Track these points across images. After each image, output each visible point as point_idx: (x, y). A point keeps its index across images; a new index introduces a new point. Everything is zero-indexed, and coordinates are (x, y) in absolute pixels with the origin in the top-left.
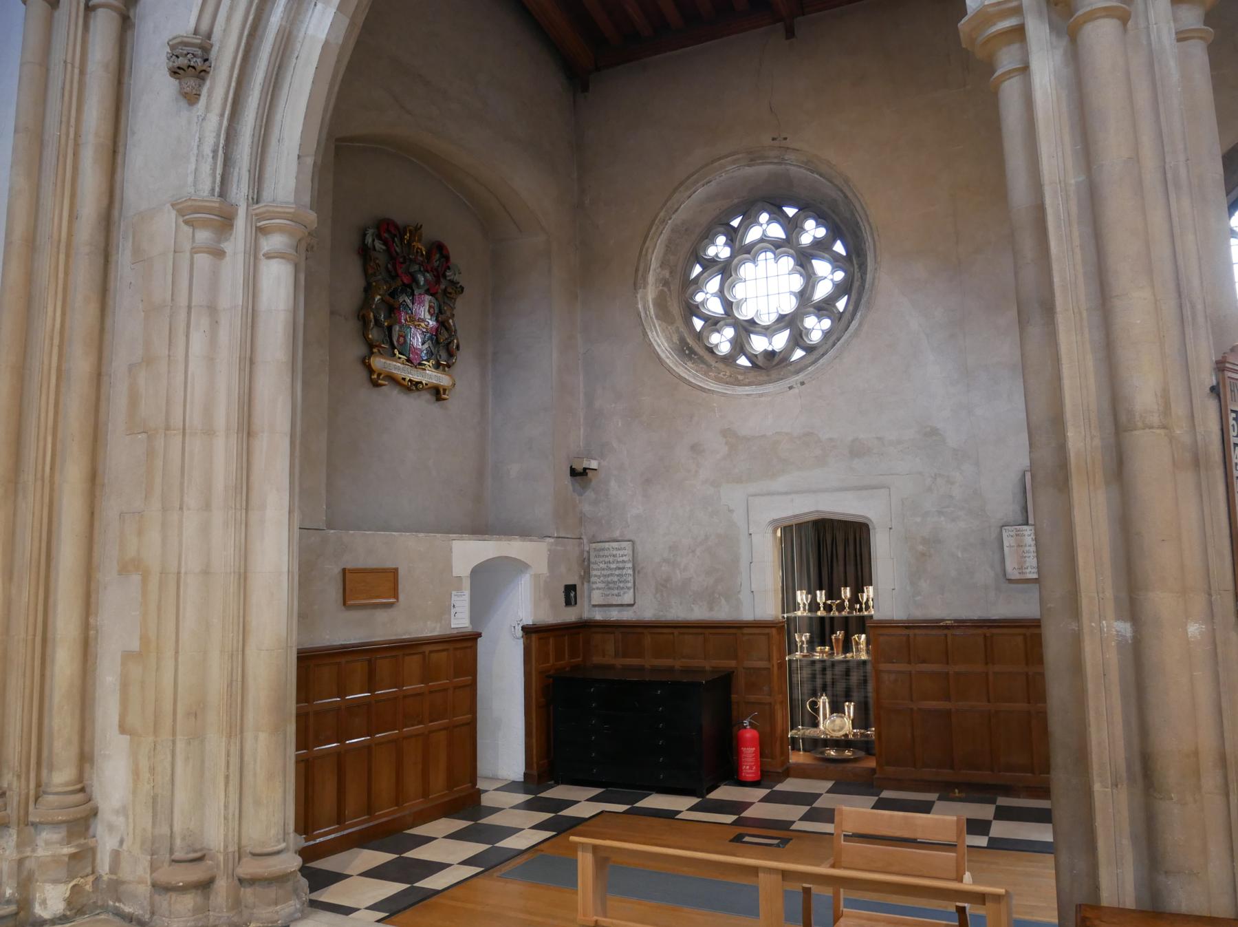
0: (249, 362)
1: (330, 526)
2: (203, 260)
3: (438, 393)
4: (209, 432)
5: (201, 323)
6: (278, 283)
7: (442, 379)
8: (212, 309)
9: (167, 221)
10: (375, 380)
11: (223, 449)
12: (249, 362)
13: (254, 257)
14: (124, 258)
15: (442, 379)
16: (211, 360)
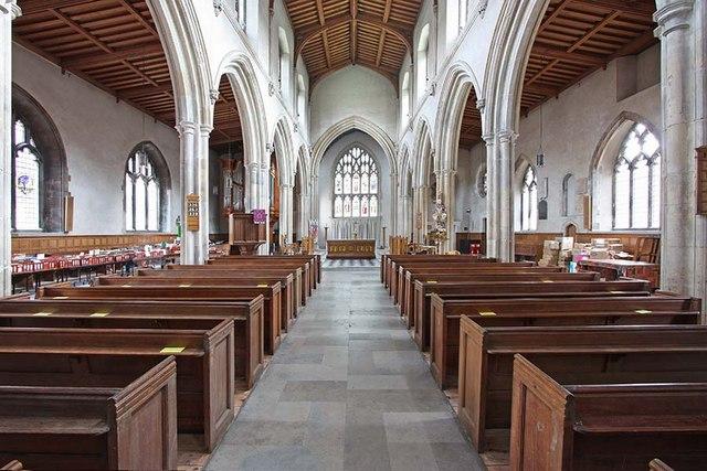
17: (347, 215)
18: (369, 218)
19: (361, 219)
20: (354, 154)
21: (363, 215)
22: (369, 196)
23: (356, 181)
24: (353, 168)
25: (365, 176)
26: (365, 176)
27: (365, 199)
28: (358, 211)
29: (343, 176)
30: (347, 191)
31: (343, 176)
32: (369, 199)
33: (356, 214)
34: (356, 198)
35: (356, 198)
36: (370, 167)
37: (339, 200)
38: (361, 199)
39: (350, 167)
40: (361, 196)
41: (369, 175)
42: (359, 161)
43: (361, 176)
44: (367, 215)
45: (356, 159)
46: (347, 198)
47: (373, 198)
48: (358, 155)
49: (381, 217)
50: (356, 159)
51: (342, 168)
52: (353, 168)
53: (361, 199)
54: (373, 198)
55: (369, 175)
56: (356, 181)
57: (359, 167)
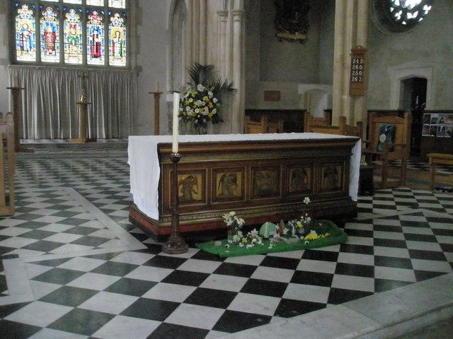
0: (232, 45)
1: (261, 80)
2: (223, 23)
3: (301, 41)
4: (224, 61)
5: (222, 37)
6: (237, 25)
7: (303, 37)
8: (225, 35)
9: (216, 15)
10: (281, 40)
11: (227, 64)
12: (232, 45)
13: (232, 22)
14: (209, 21)
15: (303, 37)
16: (225, 45)
17: (51, 58)
18: (108, 69)
19: (85, 72)
21: (93, 62)
22: (106, 13)
27: (95, 22)
28: (79, 49)
32: (107, 22)
33: (74, 59)
34: (72, 17)
35: (72, 17)
40: (85, 12)
44: (99, 62)
47: (117, 20)
49: (139, 69)
54: (117, 20)
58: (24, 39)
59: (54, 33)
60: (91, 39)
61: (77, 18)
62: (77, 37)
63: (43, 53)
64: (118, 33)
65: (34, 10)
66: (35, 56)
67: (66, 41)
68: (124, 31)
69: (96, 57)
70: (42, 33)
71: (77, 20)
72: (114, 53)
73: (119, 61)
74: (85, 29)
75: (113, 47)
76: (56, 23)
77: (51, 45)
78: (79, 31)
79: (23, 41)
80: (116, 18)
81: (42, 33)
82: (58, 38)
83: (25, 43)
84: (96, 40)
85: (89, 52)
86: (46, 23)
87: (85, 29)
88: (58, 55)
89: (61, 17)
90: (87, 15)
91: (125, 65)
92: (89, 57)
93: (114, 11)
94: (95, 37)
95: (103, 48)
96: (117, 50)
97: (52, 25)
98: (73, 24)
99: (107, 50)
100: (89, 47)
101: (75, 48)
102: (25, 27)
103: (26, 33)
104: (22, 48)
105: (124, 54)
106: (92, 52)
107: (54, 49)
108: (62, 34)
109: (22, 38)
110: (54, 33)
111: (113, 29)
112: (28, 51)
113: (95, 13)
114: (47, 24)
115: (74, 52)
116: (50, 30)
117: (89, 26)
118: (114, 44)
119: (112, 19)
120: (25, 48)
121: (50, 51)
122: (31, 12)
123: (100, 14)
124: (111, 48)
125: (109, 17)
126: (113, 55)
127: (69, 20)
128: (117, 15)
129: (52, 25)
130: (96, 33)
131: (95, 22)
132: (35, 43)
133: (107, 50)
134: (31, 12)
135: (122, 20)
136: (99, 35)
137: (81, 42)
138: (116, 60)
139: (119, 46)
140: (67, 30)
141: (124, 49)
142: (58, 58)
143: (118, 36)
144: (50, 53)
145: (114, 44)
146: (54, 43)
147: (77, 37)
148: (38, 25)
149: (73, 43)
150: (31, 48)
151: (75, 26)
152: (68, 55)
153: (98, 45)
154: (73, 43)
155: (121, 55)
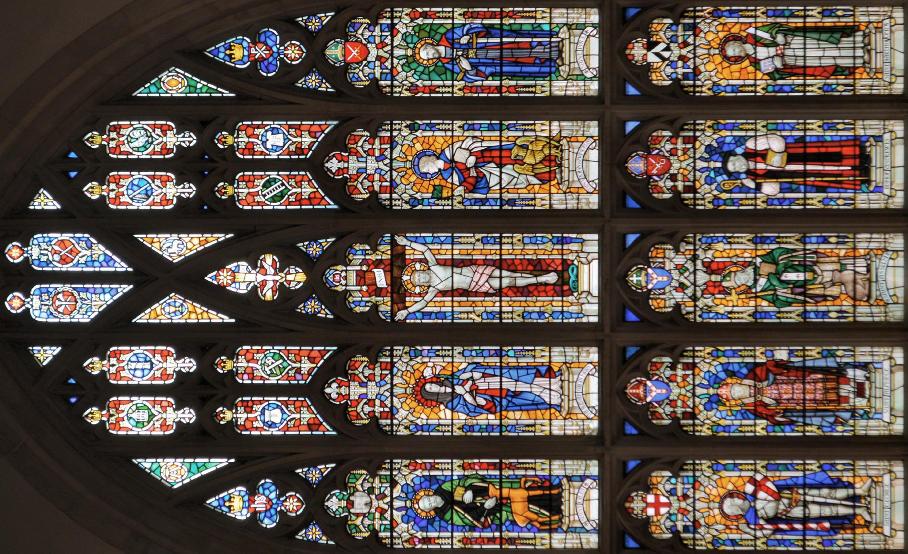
20: (93, 304)
22: (634, 109)
23: (438, 277)
24: (260, 320)
25: (400, 164)
26: (400, 164)
27: (679, 164)
28: (834, 247)
29: (365, 446)
30: (575, 392)
31: (365, 446)
32: (680, 105)
34: (666, 279)
35: (666, 279)
36: (263, 95)
37: (659, 505)
38: (678, 220)
39: (262, 363)
40: (635, 217)
41: (364, 109)
42: (174, 247)
43: (363, 218)
45: (152, 277)
46: (661, 391)
47: (660, 56)
48: (90, 253)
50: (152, 277)
51: (258, 460)
52: (260, 320)
53: (678, 220)
54: (660, 56)
55: (364, 109)
56: (438, 277)
57: (253, 235)
58: (797, 512)
59: (754, 372)
60: (770, 188)
61: (674, 259)
62: (770, 258)
63: (863, 427)
64: (732, 50)
65: (649, 464)
66: (875, 466)
67: (793, 314)
68: (716, 15)
69: (863, 165)
70: (761, 427)
71: (680, 260)
72: (837, 70)
73: (877, 40)
74: (725, 220)
75: (804, 71)
76: (707, 361)
77: (815, 390)
78: (742, 246)
79: (805, 520)
80: (652, 58)
81: (761, 427)
82: (782, 354)
83: (814, 511)
84: (776, 162)
85: (839, 200)
86: (708, 407)
87: (725, 220)
88: (863, 354)
89: (678, 333)
90: (651, 208)
91: (899, 14)
92: (864, 200)
93: (616, 66)
94: (761, 166)
95: (815, 128)
96: (817, 53)
97: (716, 381)
98: (702, 278)
99: (827, 105)
100: (815, 200)
101: (826, 271)
102: (732, 506)
103: (766, 505)
104: (840, 523)
105: (841, 17)
106: (839, 186)
107: (838, 374)
108: (755, 332)
109: (790, 521)
110: (754, 372)
111: (715, 76)
112: (855, 498)
113: (636, 165)
114: (715, 401)
115: (848, 275)
116: (740, 391)
117: (706, 195)
118: (787, 71)
119: (661, 78)
120: (842, 511)
121: (846, 390)
122: (662, 478)
123: (642, 143)
124: (815, 86)
125: (651, 94)
126: (851, 71)
127: (679, 296)
128: (637, 51)
129: (716, 381)
130: (737, 164)
131: (679, 164)
132: (813, 464)
133: (827, 105)
134: (662, 478)
135: (661, 27)
136: (750, 144)
137: (791, 241)
138: (877, 61)
139: (797, 41)
140: (735, 308)
141: (814, 15)
142: (881, 351)
143: (749, 49)
144: (860, 391)
145: (787, 71)
146: (804, 371)
147: (770, 258)
148: (726, 447)
149: (800, 276)
150: (837, 484)
151: (709, 268)
152: (863, 309)
153: (797, 152)
154: (792, 276)
155: (849, 31)
